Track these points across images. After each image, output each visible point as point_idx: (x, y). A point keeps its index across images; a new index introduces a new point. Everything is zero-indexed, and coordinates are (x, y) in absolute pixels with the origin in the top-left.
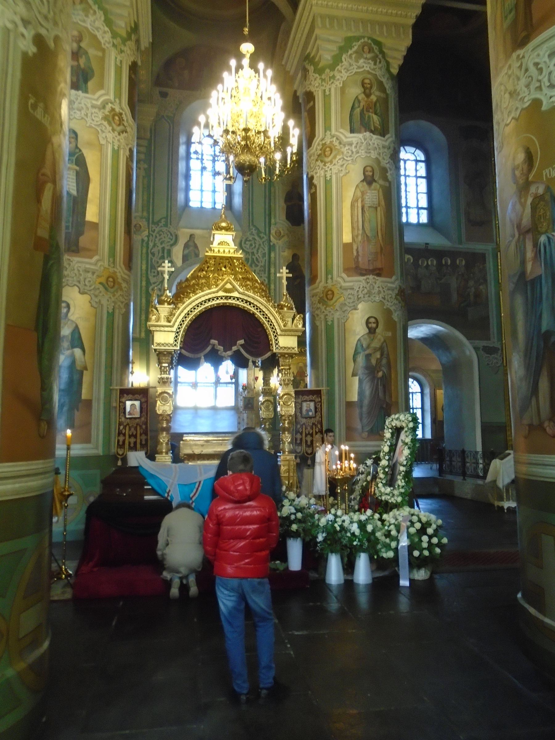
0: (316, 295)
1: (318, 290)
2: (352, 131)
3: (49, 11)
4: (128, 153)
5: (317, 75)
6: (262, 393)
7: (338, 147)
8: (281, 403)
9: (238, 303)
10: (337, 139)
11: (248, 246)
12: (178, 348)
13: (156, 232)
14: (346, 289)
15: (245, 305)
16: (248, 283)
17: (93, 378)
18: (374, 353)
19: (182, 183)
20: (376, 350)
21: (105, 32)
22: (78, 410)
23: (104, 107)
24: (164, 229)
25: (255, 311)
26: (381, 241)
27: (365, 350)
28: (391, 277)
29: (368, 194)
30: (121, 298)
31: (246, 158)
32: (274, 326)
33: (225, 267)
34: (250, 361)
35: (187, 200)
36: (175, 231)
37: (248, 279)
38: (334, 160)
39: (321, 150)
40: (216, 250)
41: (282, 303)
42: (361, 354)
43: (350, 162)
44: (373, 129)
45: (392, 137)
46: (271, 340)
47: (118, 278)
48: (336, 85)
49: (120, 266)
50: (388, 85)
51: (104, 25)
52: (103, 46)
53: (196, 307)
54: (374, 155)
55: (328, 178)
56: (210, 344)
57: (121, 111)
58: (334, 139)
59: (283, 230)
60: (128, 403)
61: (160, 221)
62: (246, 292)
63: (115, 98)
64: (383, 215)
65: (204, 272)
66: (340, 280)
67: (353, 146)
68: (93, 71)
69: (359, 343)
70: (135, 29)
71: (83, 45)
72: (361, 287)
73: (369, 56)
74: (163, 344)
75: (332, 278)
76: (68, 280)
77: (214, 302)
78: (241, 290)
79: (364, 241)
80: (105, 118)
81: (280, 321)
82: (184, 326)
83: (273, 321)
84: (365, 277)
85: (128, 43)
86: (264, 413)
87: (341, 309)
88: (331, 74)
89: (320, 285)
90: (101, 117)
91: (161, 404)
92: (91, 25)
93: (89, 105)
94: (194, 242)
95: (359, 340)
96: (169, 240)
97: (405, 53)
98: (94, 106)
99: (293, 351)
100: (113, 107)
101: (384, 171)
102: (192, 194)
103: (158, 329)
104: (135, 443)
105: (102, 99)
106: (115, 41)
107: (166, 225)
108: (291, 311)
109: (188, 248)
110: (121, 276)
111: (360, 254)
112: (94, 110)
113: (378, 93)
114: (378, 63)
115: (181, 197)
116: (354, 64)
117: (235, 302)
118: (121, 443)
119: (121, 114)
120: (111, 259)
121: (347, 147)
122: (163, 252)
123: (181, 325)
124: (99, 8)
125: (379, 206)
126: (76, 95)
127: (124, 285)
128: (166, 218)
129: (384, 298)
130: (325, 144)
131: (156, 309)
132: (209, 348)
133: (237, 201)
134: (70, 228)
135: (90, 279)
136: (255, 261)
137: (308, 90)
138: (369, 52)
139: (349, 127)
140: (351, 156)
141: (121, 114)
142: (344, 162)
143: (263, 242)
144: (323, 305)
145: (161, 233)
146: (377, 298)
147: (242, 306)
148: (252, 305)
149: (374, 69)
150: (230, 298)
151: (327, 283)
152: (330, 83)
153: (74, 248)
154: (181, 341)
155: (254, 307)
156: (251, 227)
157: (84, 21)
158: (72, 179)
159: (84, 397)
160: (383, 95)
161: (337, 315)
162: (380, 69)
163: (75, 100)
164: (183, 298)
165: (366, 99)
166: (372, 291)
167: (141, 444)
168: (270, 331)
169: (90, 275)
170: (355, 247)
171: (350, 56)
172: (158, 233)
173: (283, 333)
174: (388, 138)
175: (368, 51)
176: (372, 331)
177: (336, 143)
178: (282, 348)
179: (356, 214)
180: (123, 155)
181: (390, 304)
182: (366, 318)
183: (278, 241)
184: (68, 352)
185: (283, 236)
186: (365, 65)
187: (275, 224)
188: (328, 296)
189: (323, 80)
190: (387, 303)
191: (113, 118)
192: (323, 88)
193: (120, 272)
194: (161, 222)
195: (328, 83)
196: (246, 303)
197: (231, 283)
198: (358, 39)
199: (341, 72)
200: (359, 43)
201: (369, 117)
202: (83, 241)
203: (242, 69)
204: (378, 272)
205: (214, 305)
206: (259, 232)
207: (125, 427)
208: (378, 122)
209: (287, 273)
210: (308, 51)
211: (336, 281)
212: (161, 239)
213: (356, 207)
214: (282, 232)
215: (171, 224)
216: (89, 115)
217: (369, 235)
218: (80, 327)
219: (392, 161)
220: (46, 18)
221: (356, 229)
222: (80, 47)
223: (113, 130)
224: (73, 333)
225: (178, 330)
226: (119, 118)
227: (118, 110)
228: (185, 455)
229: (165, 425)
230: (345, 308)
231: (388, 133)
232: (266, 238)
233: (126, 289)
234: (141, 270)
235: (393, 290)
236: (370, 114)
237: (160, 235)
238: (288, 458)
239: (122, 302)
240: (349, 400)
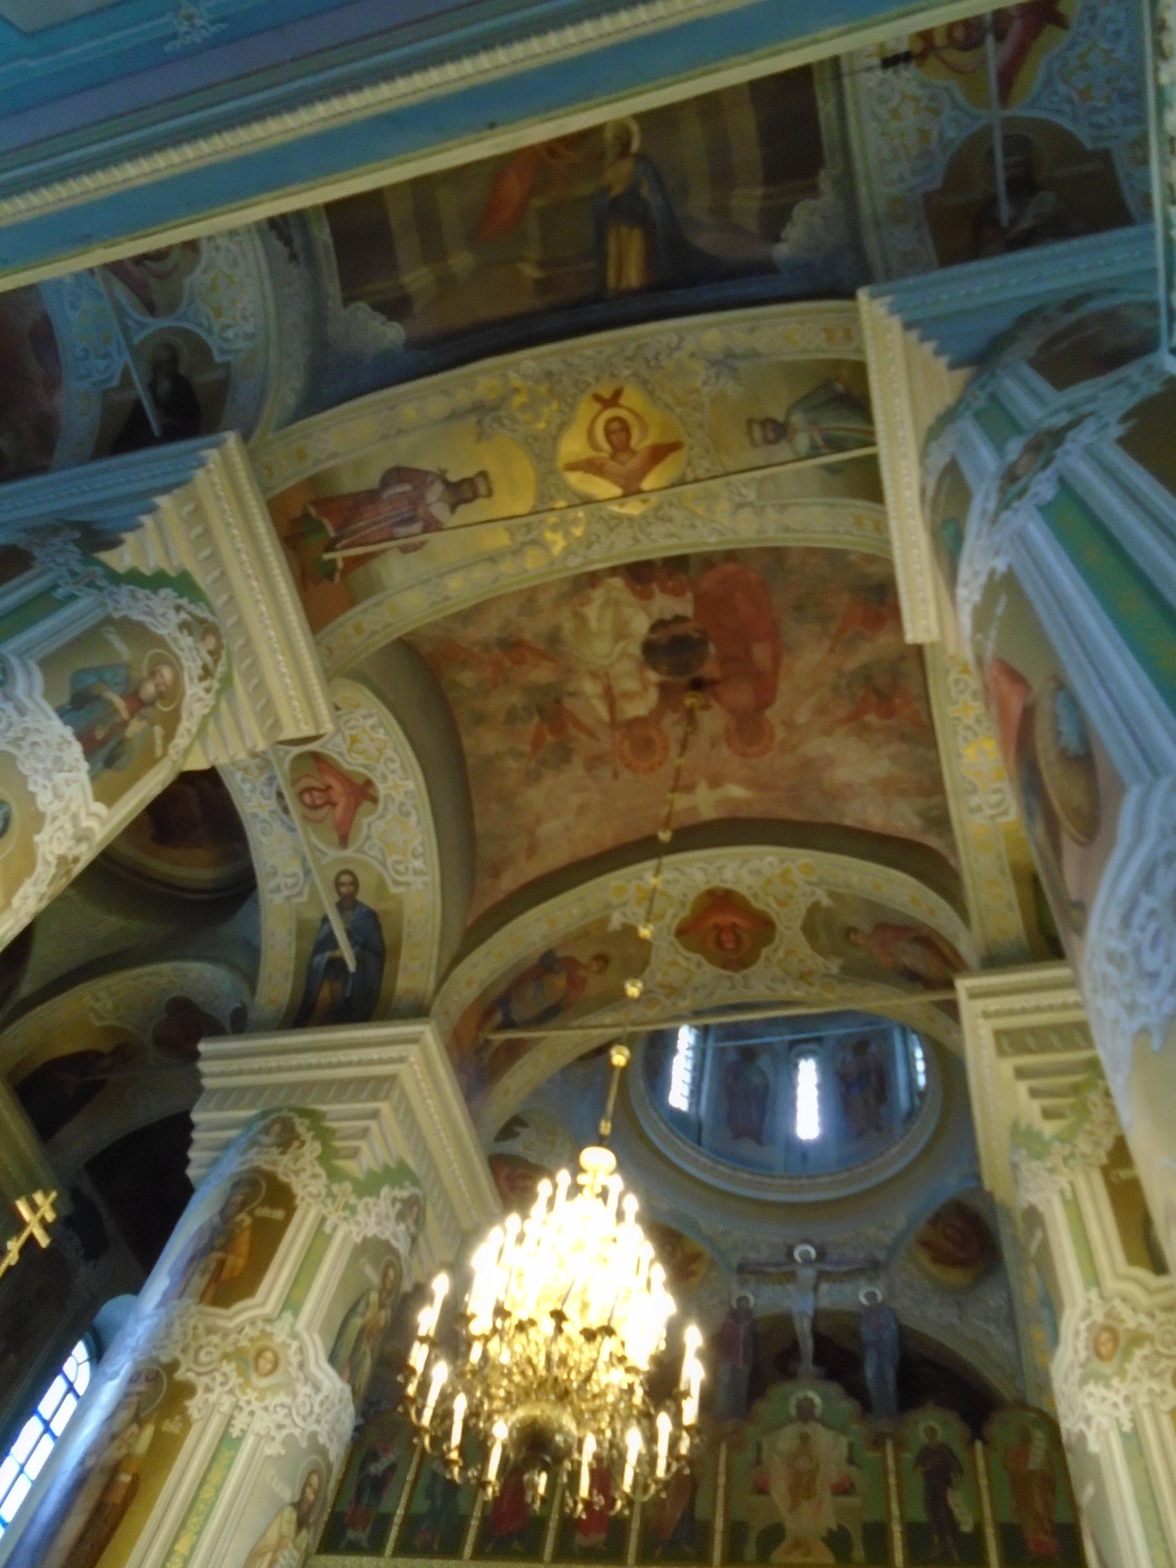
2: (332, 1359)
10: (301, 1350)
29: (286, 1553)
48: (351, 1232)
55: (235, 1432)
58: (295, 1345)
93: (73, 808)
98: (75, 818)
116: (393, 1221)
126: (77, 760)
130: (270, 1336)
140: (304, 1419)
142: (287, 1422)
152: (341, 1214)
157: (191, 679)
163: (66, 768)
189: (330, 1194)
192: (324, 1212)
195: (337, 1210)
198: (415, 1182)
216: (57, 824)
222: (152, 703)
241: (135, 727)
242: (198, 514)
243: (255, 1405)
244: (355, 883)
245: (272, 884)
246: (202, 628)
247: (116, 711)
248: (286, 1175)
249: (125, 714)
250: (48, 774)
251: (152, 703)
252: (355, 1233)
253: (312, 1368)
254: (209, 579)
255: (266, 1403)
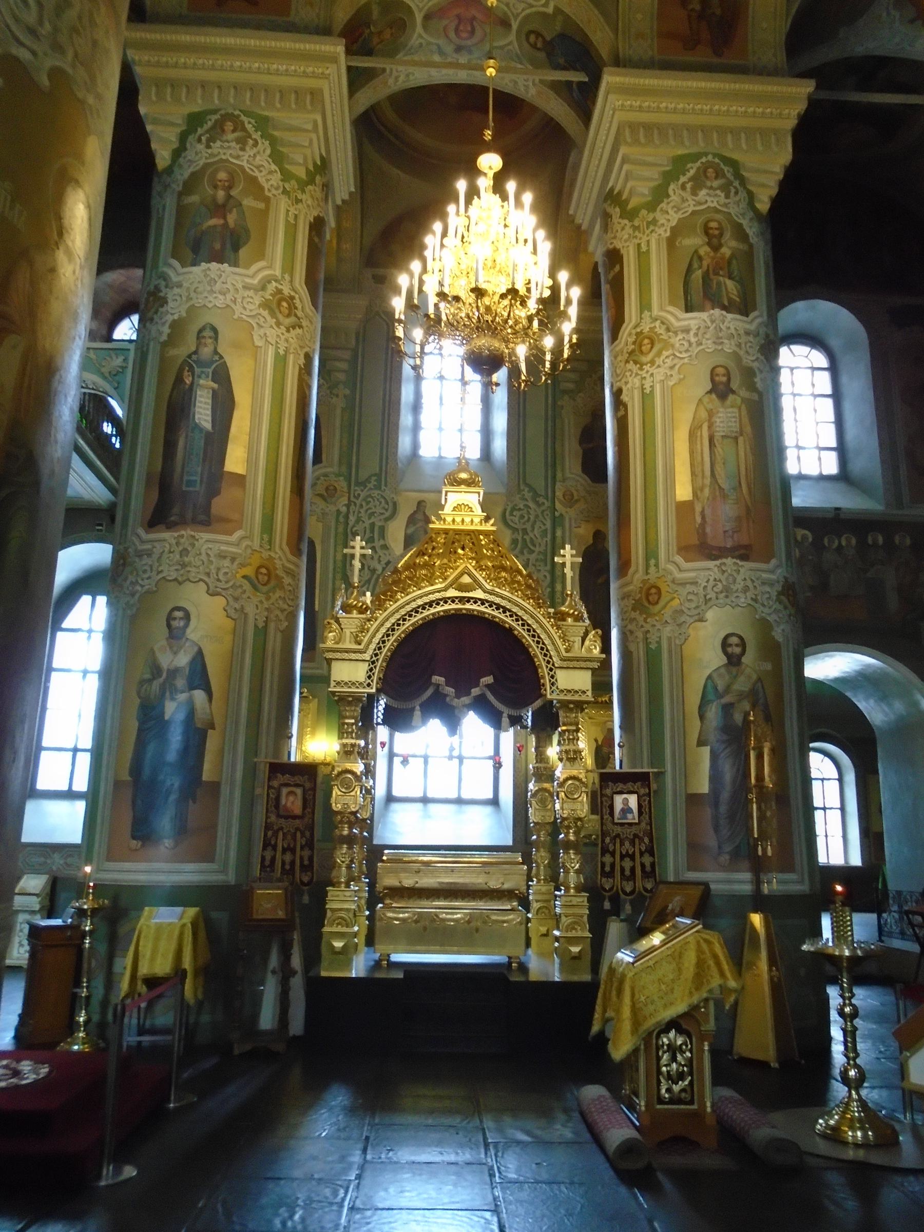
0: (629, 596)
1: (631, 587)
2: (689, 308)
3: (41, 22)
4: (302, 361)
5: (626, 221)
6: (534, 775)
7: (664, 337)
8: (562, 795)
9: (482, 608)
10: (663, 323)
11: (516, 519)
12: (374, 690)
13: (361, 498)
14: (683, 584)
15: (496, 613)
16: (503, 574)
17: (224, 743)
18: (739, 701)
19: (406, 419)
20: (741, 696)
21: (271, 172)
22: (194, 802)
23: (263, 288)
24: (376, 493)
25: (514, 624)
26: (747, 497)
27: (721, 696)
28: (768, 562)
30: (281, 602)
31: (484, 342)
32: (547, 650)
33: (463, 549)
34: (505, 715)
35: (416, 446)
36: (392, 495)
37: (503, 568)
38: (656, 359)
39: (634, 343)
40: (449, 519)
41: (563, 608)
42: (715, 703)
43: (686, 361)
44: (726, 303)
45: (761, 316)
46: (543, 677)
47: (276, 569)
49: (281, 549)
50: (752, 230)
51: (270, 160)
52: (267, 193)
53: (407, 617)
54: (729, 347)
55: (648, 391)
56: (431, 684)
57: (293, 294)
58: (658, 323)
59: (577, 491)
60: (285, 791)
61: (368, 480)
62: (497, 590)
63: (283, 273)
64: (748, 450)
65: (426, 557)
66: (671, 567)
67: (692, 333)
68: (247, 231)
69: (710, 683)
70: (323, 166)
71: (233, 193)
72: (712, 579)
73: (716, 184)
74: (346, 683)
75: (657, 565)
76: (189, 571)
77: (439, 608)
78: (488, 587)
79: (714, 498)
80: (265, 305)
81: (559, 642)
82: (385, 651)
83: (546, 642)
84: (718, 562)
85: (310, 187)
86: (537, 813)
87: (674, 619)
88: (651, 217)
89: (637, 576)
90: (257, 303)
91: (339, 793)
92: (248, 161)
93: (239, 286)
94: (424, 513)
95: (710, 677)
96: (384, 511)
97: (781, 177)
98: (246, 287)
99: (584, 698)
100: (280, 287)
101: (749, 374)
102: (423, 436)
103: (338, 655)
104: (293, 863)
105: (260, 276)
106: (287, 186)
107: (378, 487)
108: (581, 624)
109: (415, 524)
110: (283, 565)
111: (708, 519)
112: (246, 293)
113: (733, 244)
114: (732, 194)
115: (404, 442)
117: (478, 608)
118: (267, 863)
119: (292, 298)
120: (265, 536)
121: (680, 336)
122: (372, 531)
123: (380, 648)
124: (262, 137)
125: (742, 435)
127: (287, 580)
128: (379, 476)
129: (755, 600)
130: (641, 332)
131: (337, 621)
132: (429, 692)
133: (500, 446)
134: (199, 482)
135: (226, 570)
136: (529, 545)
137: (611, 247)
138: (716, 178)
139: (683, 302)
140: (687, 351)
141: (292, 298)
142: (676, 361)
143: (543, 512)
144: (641, 614)
145: (369, 499)
146: (743, 600)
147: (489, 614)
148: (508, 614)
149: (726, 205)
150: (468, 601)
151: (647, 573)
152: (647, 232)
153: (202, 517)
154: (380, 679)
155: (511, 616)
156: (522, 488)
157: (238, 157)
158: (205, 403)
159: (205, 777)
160: (743, 247)
161: (667, 631)
162: (738, 203)
164: (385, 600)
165: (712, 254)
166: (732, 586)
167: (302, 865)
168: (540, 660)
169: (227, 563)
170: (698, 508)
171: (683, 187)
172: (364, 500)
173: (565, 664)
174: (756, 318)
175: (714, 175)
176: (733, 661)
177: (660, 330)
178: (562, 691)
179: (699, 450)
180: (294, 363)
181: (766, 610)
182: (722, 635)
183: (568, 509)
184: (182, 697)
185: (577, 501)
186: (709, 199)
187: (564, 480)
188: (651, 598)
189: (636, 228)
190: (762, 608)
191: (279, 305)
192: (637, 241)
193: (280, 558)
194: (370, 482)
195: (644, 233)
196: (497, 609)
197: (470, 575)
199: (667, 213)
200: (698, 164)
201: (719, 284)
202: (218, 505)
203: (479, 197)
204: (742, 551)
205: (438, 612)
206: (536, 495)
207: (276, 834)
208: (735, 293)
209: (572, 556)
210: (610, 185)
211: (664, 570)
212: (370, 508)
213: (699, 439)
214: (575, 494)
215: (386, 486)
217: (723, 486)
218: (206, 652)
219: (762, 358)
220: (32, 32)
221: (700, 475)
222: (229, 197)
223: (278, 324)
224: (193, 662)
225: (374, 659)
226: (289, 305)
227: (286, 291)
228: (386, 888)
229: (346, 832)
230: (683, 619)
231: (754, 309)
232: (547, 504)
233: (290, 588)
234: (335, 562)
235: (771, 585)
236: (721, 279)
237: (368, 503)
238: (575, 901)
239: (283, 611)
240: (692, 790)
241: (232, 218)
242: (159, 84)
243: (651, 370)
244: (538, 34)
245: (522, 89)
246: (217, 131)
247: (215, 226)
248: (611, 243)
249: (221, 221)
250: (212, 292)
251: (229, 197)
252: (663, 233)
253: (676, 324)
254: (200, 101)
255: (657, 363)
